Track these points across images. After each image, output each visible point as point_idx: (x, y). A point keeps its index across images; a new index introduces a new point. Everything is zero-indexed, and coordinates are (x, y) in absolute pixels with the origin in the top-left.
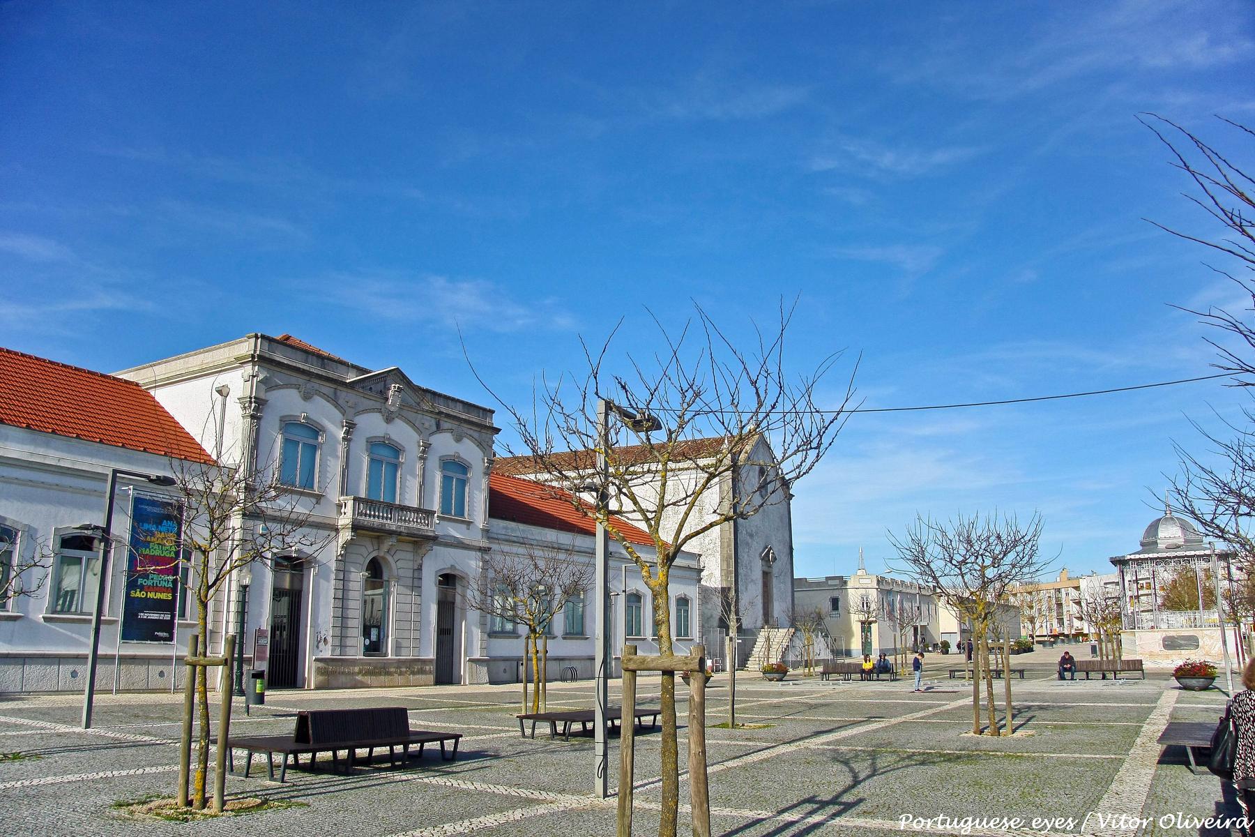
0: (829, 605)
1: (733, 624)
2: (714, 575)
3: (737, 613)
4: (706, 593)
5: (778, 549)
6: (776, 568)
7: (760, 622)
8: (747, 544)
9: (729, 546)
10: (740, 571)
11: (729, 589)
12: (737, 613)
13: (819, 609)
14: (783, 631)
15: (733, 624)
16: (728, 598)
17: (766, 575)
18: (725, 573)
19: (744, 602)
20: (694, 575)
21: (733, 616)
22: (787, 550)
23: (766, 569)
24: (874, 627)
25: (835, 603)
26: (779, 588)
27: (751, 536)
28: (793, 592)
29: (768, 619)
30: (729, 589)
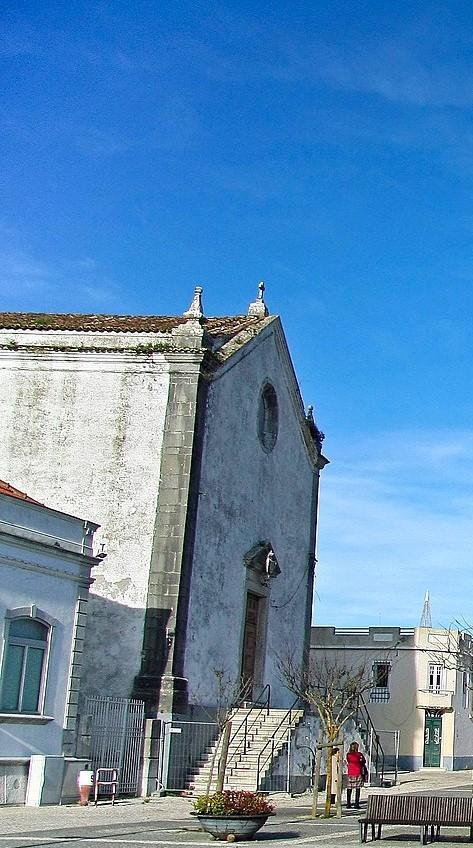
0: (371, 675)
1: (167, 691)
2: (129, 577)
3: (178, 670)
4: (103, 618)
5: (280, 552)
6: (277, 590)
7: (232, 691)
8: (218, 527)
9: (174, 522)
10: (195, 579)
11: (168, 612)
12: (178, 670)
13: (348, 681)
14: (277, 715)
15: (167, 691)
16: (163, 637)
17: (254, 600)
18: (158, 581)
19: (197, 643)
20: (75, 568)
21: (168, 677)
22: (303, 561)
23: (256, 588)
24: (448, 719)
25: (383, 671)
26: (276, 630)
27: (230, 513)
28: (307, 648)
29: (250, 694)
30: (168, 612)
